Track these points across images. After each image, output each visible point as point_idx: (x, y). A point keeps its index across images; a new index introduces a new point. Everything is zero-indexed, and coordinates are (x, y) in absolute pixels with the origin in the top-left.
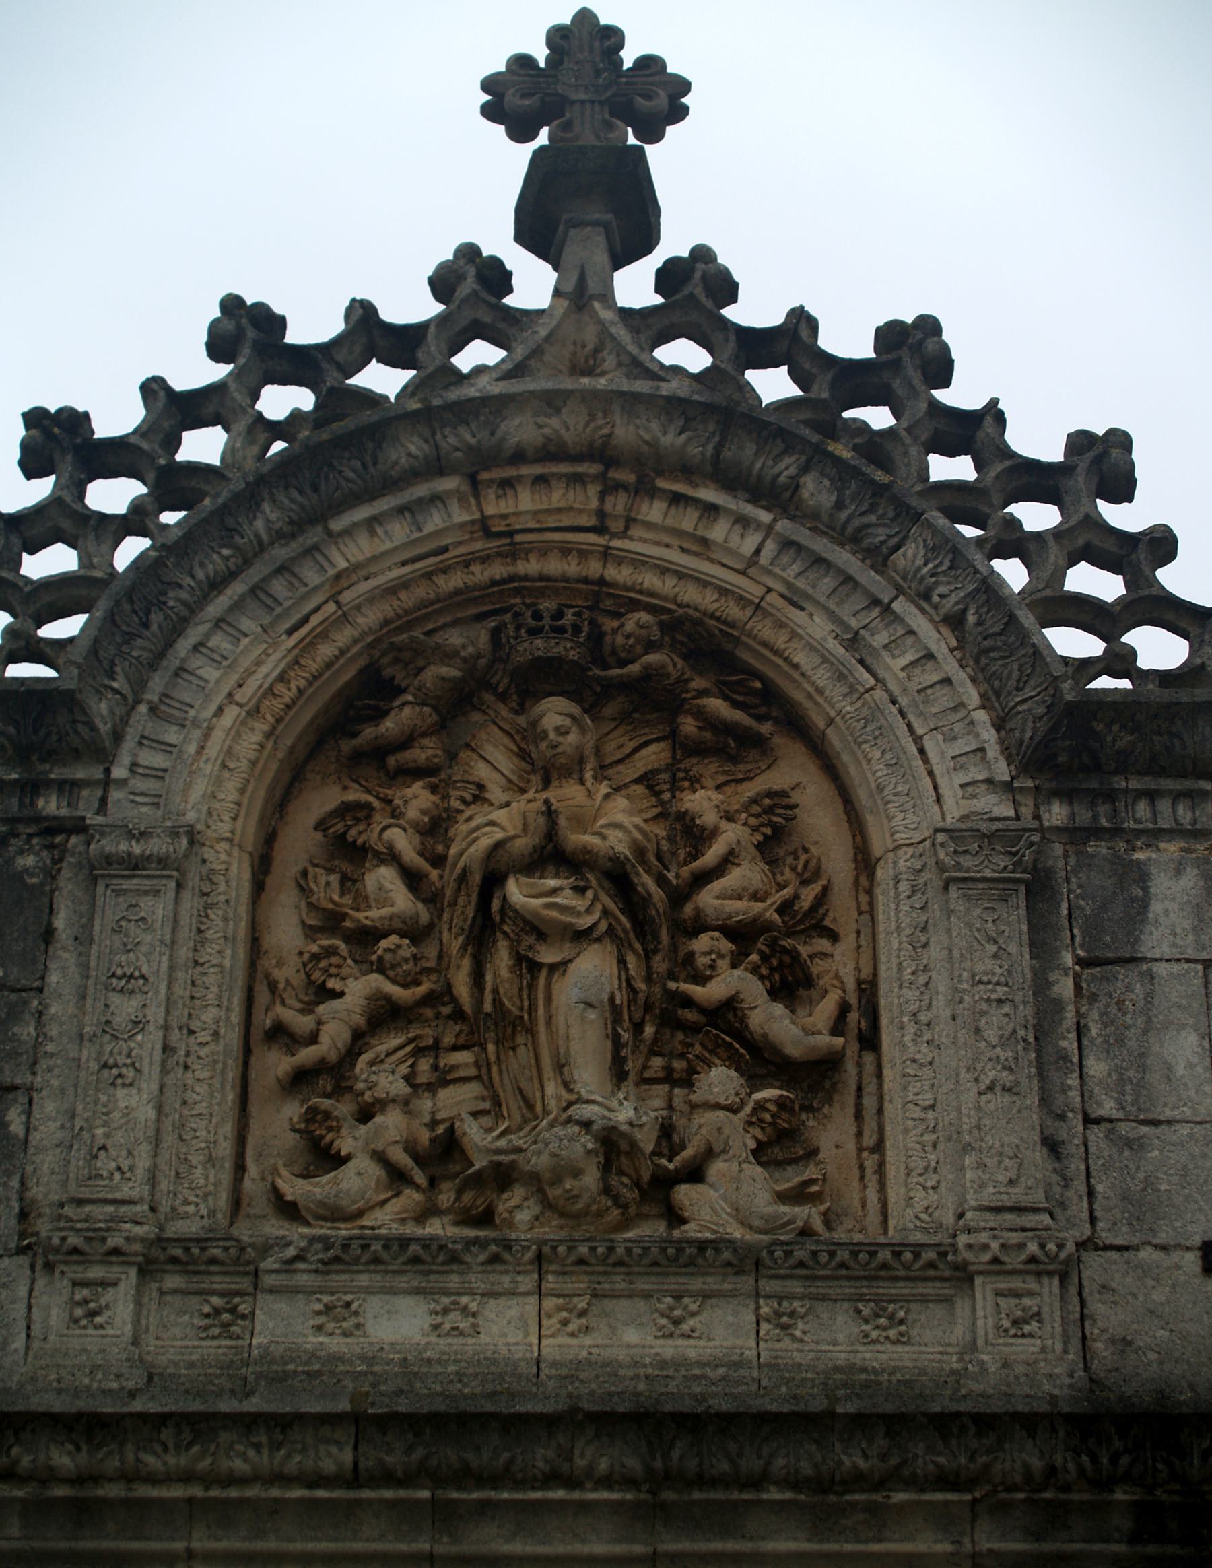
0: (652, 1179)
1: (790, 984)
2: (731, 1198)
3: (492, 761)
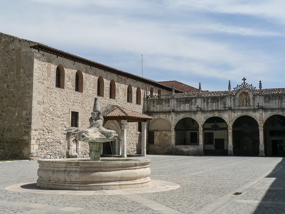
0: (246, 105)
1: (249, 100)
2: (248, 105)
3: (243, 95)
